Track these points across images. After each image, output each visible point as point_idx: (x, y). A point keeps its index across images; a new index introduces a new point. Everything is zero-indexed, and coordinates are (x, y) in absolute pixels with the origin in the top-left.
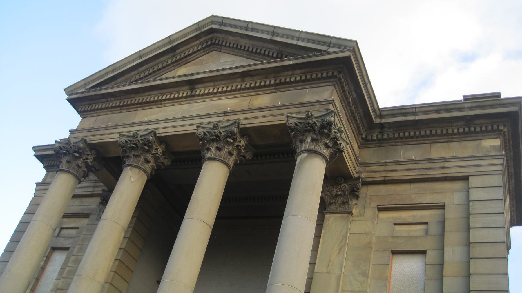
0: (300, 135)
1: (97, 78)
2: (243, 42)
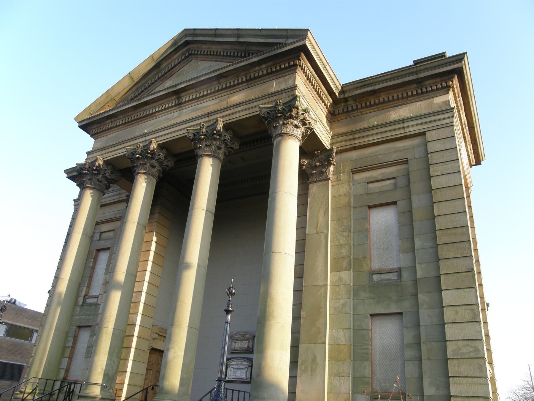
0: (273, 122)
2: (214, 48)
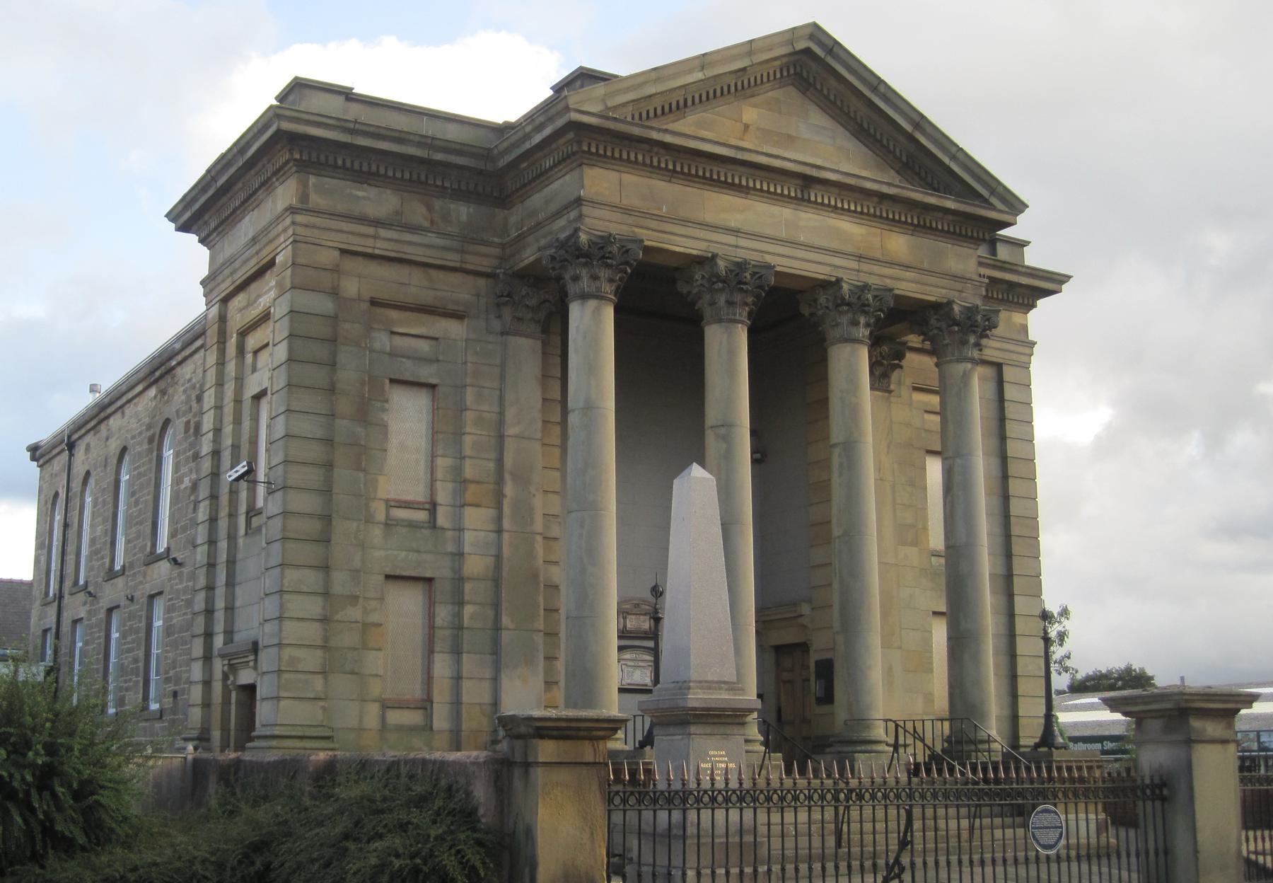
1: (628, 88)
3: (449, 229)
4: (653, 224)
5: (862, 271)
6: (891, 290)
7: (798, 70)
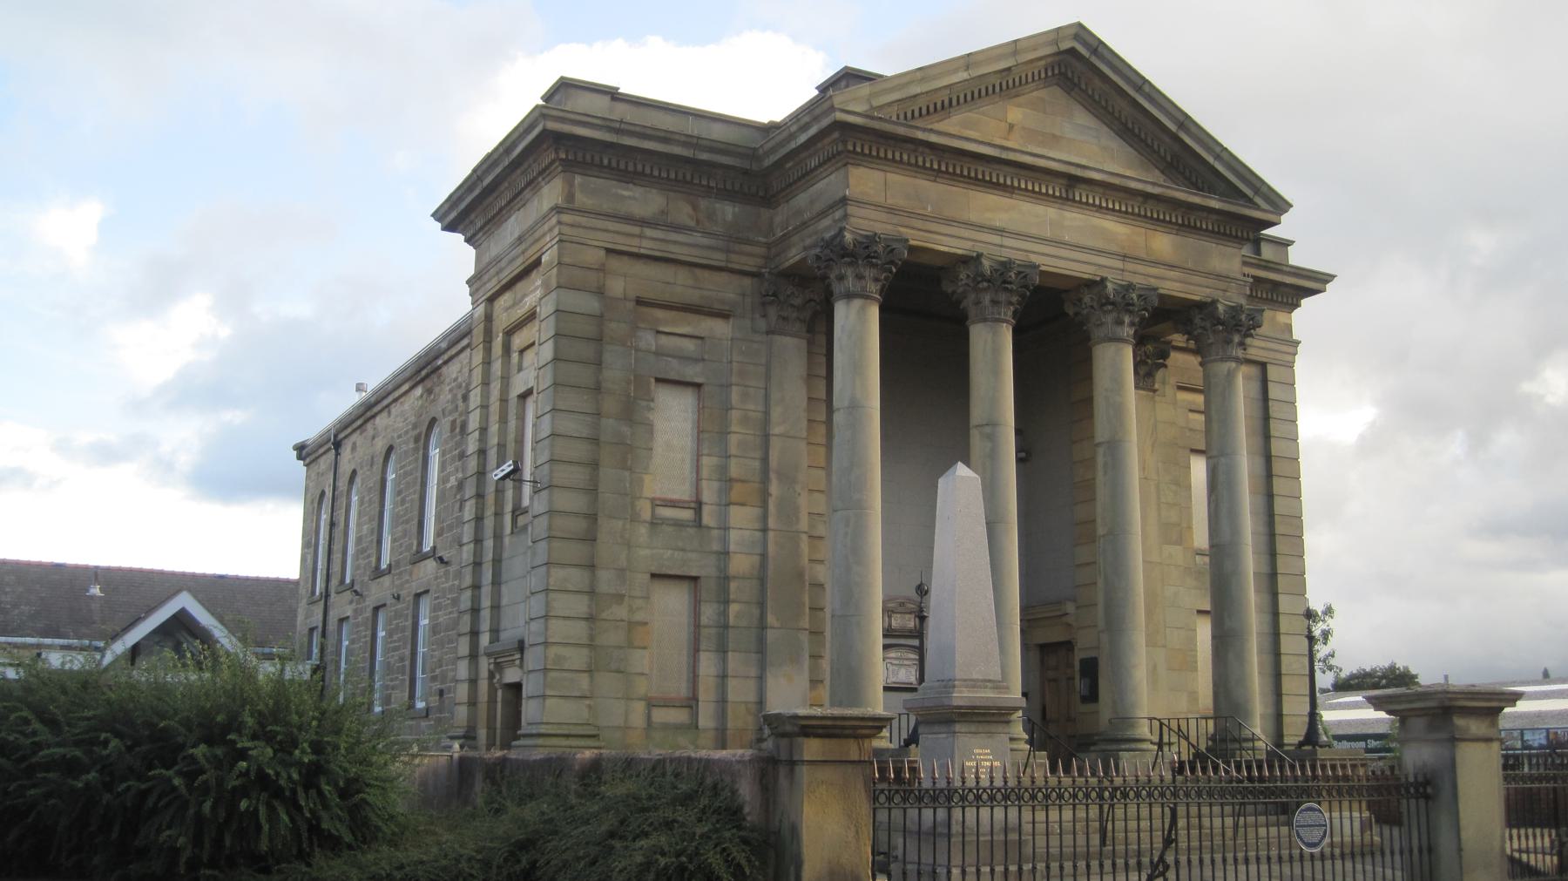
3: (715, 228)
4: (918, 224)
5: (1126, 271)
6: (1155, 289)
7: (1063, 70)
